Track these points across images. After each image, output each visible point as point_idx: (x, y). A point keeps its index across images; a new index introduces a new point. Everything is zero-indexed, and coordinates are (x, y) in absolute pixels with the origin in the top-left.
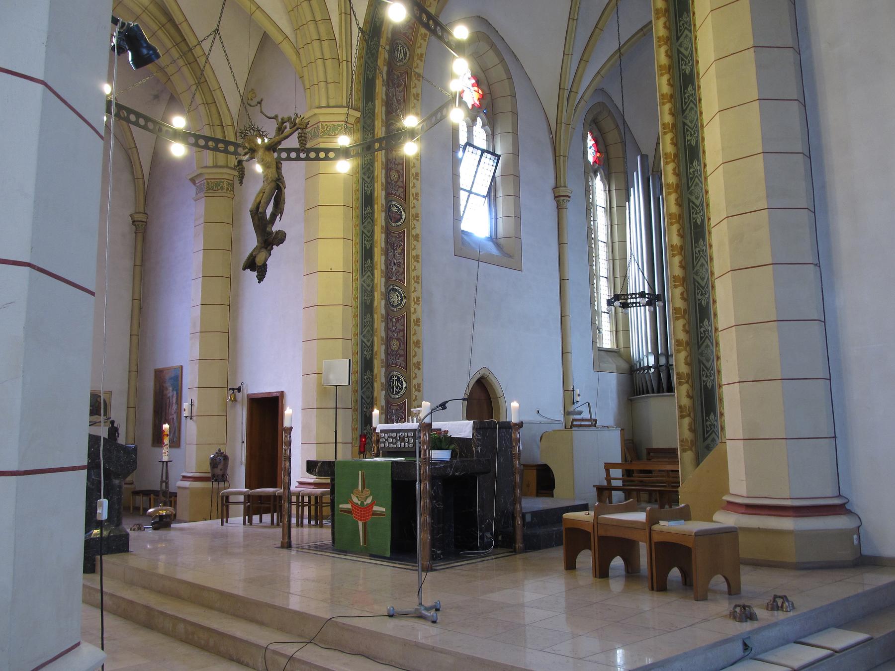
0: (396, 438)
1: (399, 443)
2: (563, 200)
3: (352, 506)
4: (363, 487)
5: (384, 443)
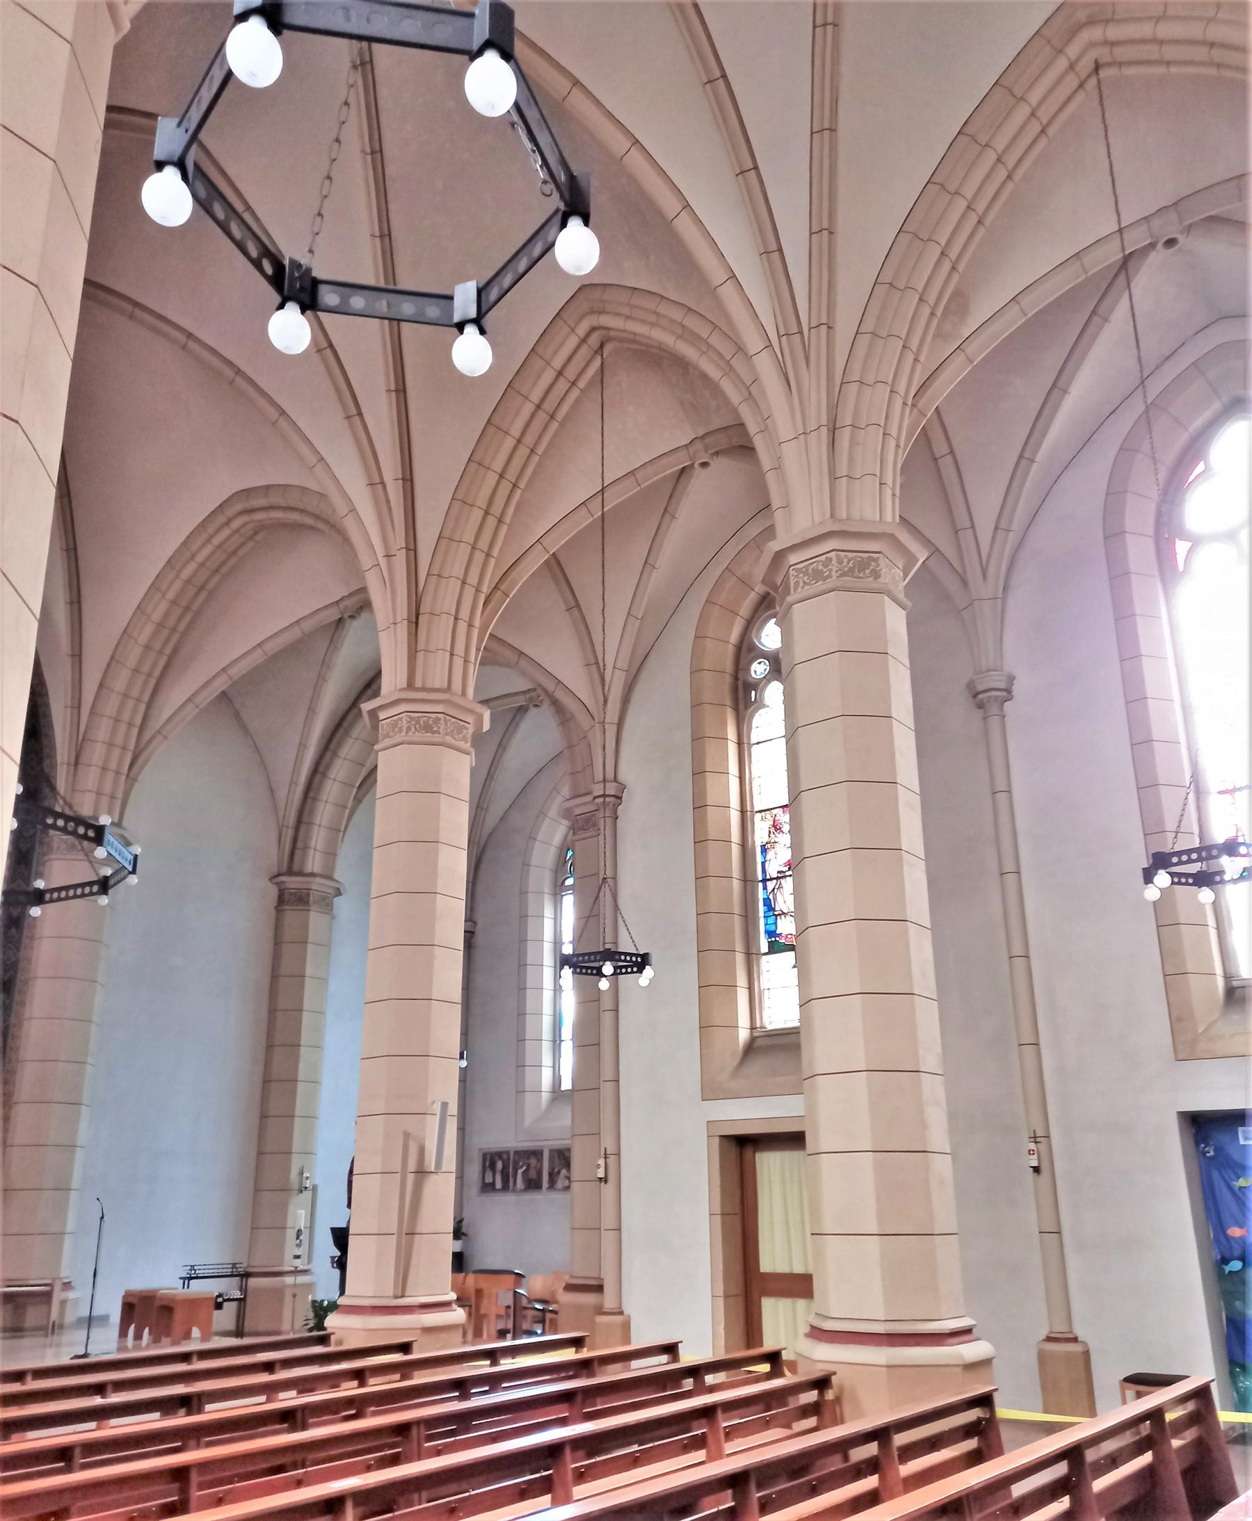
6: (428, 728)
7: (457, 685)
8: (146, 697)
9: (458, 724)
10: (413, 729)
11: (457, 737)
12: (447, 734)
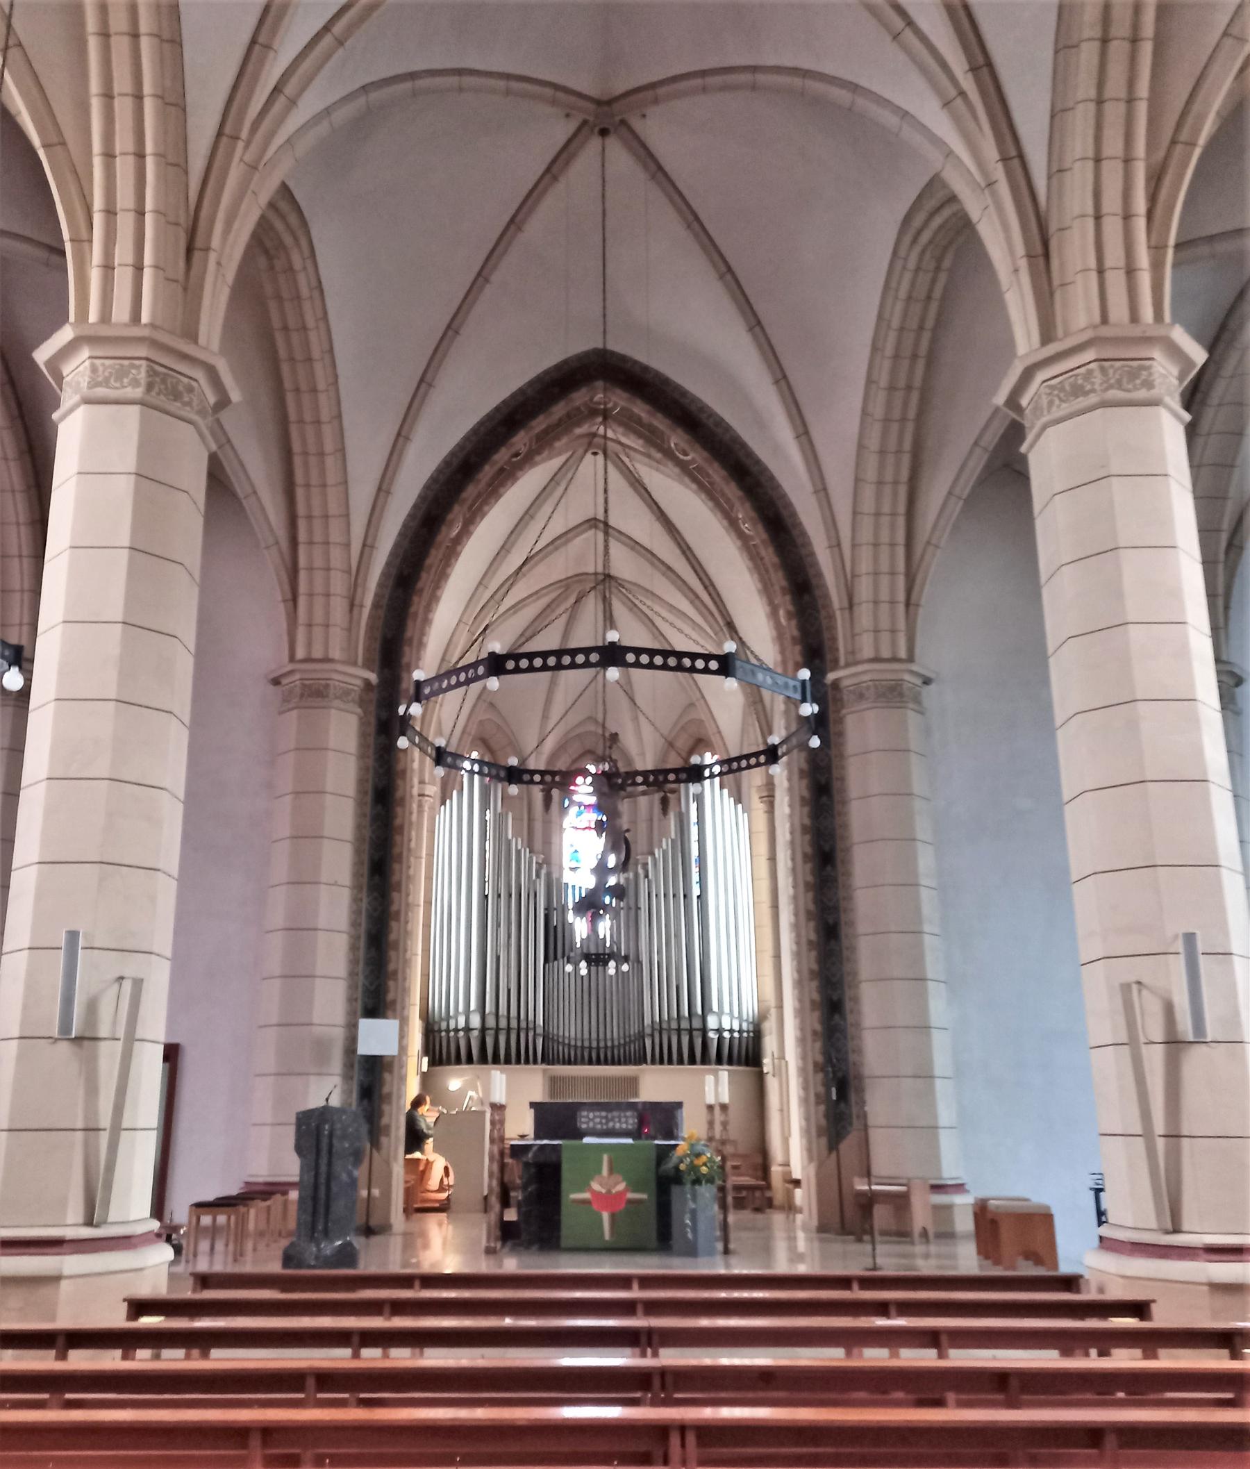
0: (606, 1117)
1: (611, 1124)
2: (426, 801)
3: (592, 1196)
4: (611, 1171)
5: (587, 1123)
6: (1078, 391)
7: (1118, 310)
8: (902, 508)
9: (1128, 366)
10: (1057, 402)
11: (1130, 386)
12: (1111, 387)
